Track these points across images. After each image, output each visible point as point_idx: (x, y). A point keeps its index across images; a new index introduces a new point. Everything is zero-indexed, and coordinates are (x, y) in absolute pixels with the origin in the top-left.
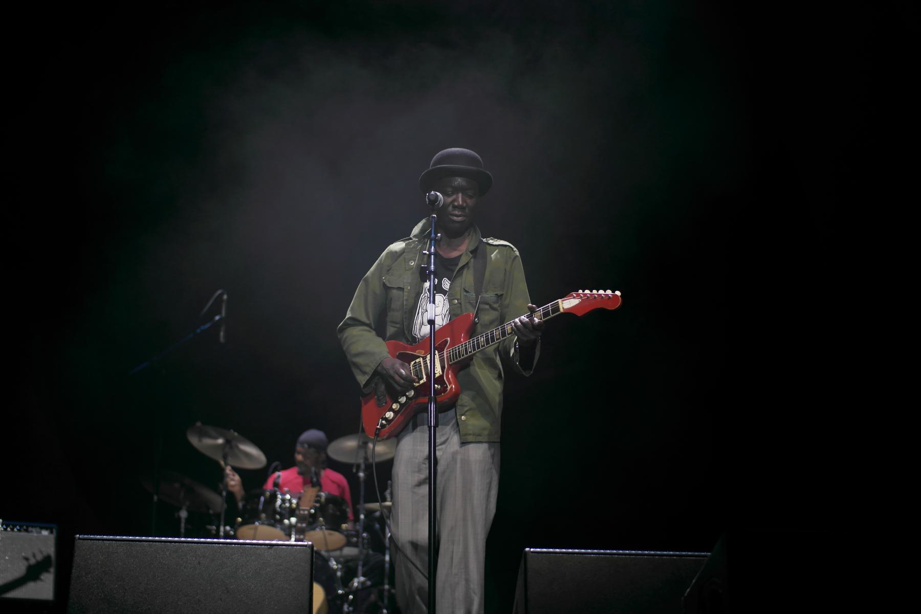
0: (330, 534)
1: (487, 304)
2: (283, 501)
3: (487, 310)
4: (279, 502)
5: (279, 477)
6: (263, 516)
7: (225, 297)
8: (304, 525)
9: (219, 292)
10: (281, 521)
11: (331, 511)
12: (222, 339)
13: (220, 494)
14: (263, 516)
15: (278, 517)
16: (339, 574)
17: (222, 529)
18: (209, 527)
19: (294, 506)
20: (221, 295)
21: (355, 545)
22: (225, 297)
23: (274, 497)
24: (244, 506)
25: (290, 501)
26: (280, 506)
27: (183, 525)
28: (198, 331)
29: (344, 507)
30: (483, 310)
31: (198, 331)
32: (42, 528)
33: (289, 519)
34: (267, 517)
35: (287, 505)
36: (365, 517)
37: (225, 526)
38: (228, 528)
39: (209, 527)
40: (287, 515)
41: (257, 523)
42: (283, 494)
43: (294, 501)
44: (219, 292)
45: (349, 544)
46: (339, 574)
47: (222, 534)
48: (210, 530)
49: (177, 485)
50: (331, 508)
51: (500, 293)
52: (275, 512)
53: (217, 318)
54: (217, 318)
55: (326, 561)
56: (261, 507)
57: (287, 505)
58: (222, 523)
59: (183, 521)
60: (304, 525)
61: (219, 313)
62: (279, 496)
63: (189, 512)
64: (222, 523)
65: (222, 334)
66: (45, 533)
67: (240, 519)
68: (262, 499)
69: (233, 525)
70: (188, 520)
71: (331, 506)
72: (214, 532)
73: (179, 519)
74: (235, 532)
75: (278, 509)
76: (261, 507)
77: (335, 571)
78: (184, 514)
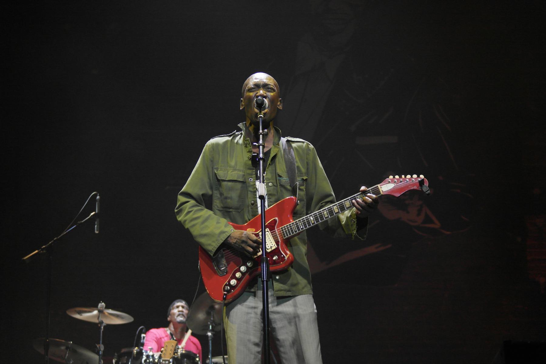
2: (148, 356)
5: (144, 337)
19: (156, 361)
23: (140, 354)
25: (153, 356)
26: (145, 361)
35: (151, 360)
57: (151, 360)
62: (144, 354)
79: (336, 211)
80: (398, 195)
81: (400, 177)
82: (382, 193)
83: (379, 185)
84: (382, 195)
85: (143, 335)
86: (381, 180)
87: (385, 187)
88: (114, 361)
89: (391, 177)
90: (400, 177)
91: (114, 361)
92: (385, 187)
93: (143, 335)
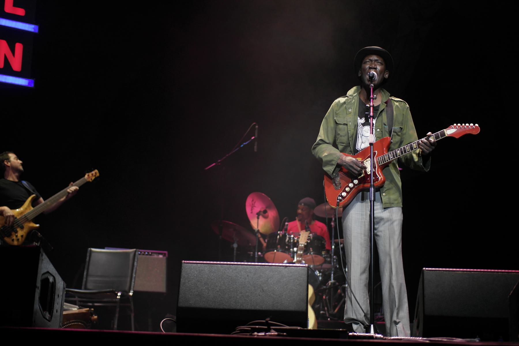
0: (315, 257)
2: (290, 238)
4: (287, 239)
7: (257, 127)
8: (302, 252)
9: (254, 123)
10: (288, 250)
12: (255, 150)
15: (287, 247)
16: (320, 278)
17: (256, 253)
18: (249, 253)
20: (255, 125)
21: (330, 262)
22: (257, 127)
23: (284, 236)
26: (288, 241)
27: (235, 252)
28: (242, 146)
31: (242, 146)
33: (293, 249)
34: (281, 247)
36: (335, 247)
37: (258, 252)
38: (260, 253)
39: (249, 253)
40: (292, 247)
42: (290, 235)
43: (296, 239)
44: (254, 123)
45: (325, 262)
46: (320, 278)
48: (250, 254)
53: (253, 138)
54: (253, 138)
59: (235, 249)
60: (302, 252)
65: (255, 147)
66: (161, 256)
68: (278, 237)
70: (238, 248)
73: (233, 248)
76: (277, 241)
77: (318, 277)
78: (235, 246)
79: (415, 147)
80: (457, 137)
81: (461, 125)
82: (446, 135)
83: (445, 130)
84: (447, 137)
85: (286, 223)
86: (447, 126)
87: (449, 132)
89: (455, 125)
90: (461, 125)
92: (449, 132)
93: (286, 223)
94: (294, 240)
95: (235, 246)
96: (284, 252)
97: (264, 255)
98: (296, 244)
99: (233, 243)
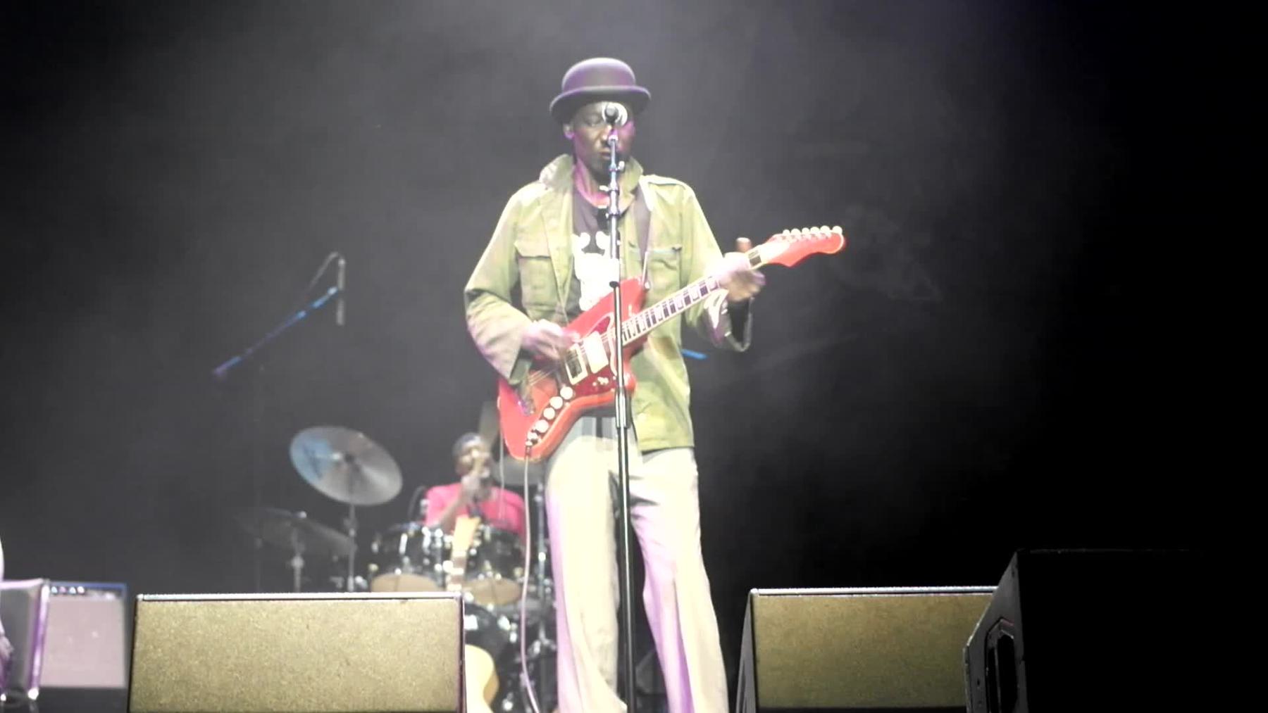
1: (662, 261)
2: (433, 539)
3: (661, 269)
4: (426, 543)
6: (406, 560)
7: (342, 262)
10: (431, 568)
11: (499, 551)
13: (346, 533)
14: (406, 560)
15: (427, 561)
20: (336, 260)
22: (342, 262)
23: (419, 535)
24: (381, 548)
26: (430, 548)
29: (517, 546)
30: (654, 270)
32: (106, 590)
37: (355, 576)
40: (439, 559)
41: (398, 571)
42: (433, 530)
44: (333, 255)
47: (351, 586)
49: (288, 524)
50: (499, 548)
51: (677, 246)
52: (422, 555)
53: (332, 291)
54: (332, 291)
55: (494, 620)
56: (403, 549)
58: (351, 572)
61: (334, 284)
63: (304, 557)
64: (351, 572)
66: (109, 597)
67: (374, 567)
69: (365, 574)
70: (304, 571)
71: (499, 544)
72: (340, 585)
73: (292, 570)
74: (369, 583)
75: (427, 552)
76: (403, 549)
78: (298, 563)
88: (375, 547)
91: (375, 547)
94: (443, 543)
95: (298, 563)
96: (420, 573)
97: (369, 583)
98: (446, 554)
99: (292, 555)
